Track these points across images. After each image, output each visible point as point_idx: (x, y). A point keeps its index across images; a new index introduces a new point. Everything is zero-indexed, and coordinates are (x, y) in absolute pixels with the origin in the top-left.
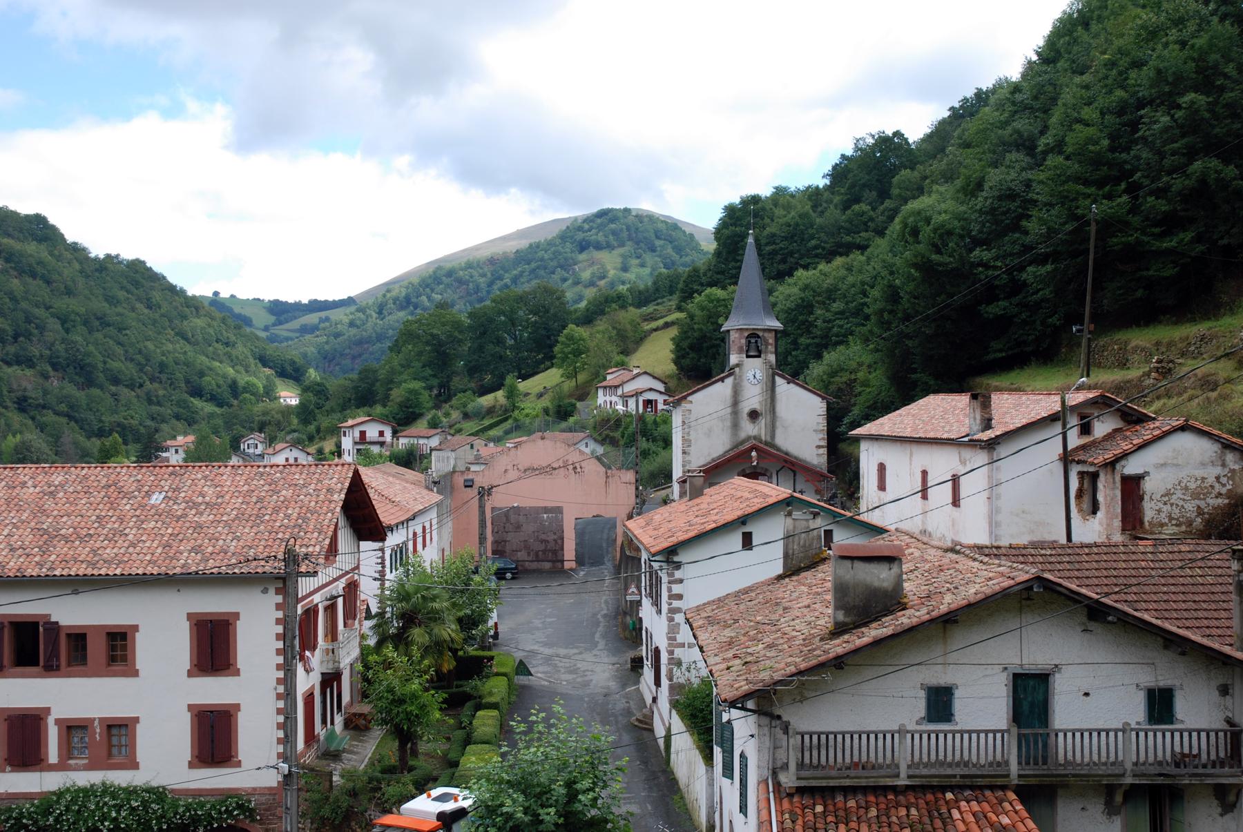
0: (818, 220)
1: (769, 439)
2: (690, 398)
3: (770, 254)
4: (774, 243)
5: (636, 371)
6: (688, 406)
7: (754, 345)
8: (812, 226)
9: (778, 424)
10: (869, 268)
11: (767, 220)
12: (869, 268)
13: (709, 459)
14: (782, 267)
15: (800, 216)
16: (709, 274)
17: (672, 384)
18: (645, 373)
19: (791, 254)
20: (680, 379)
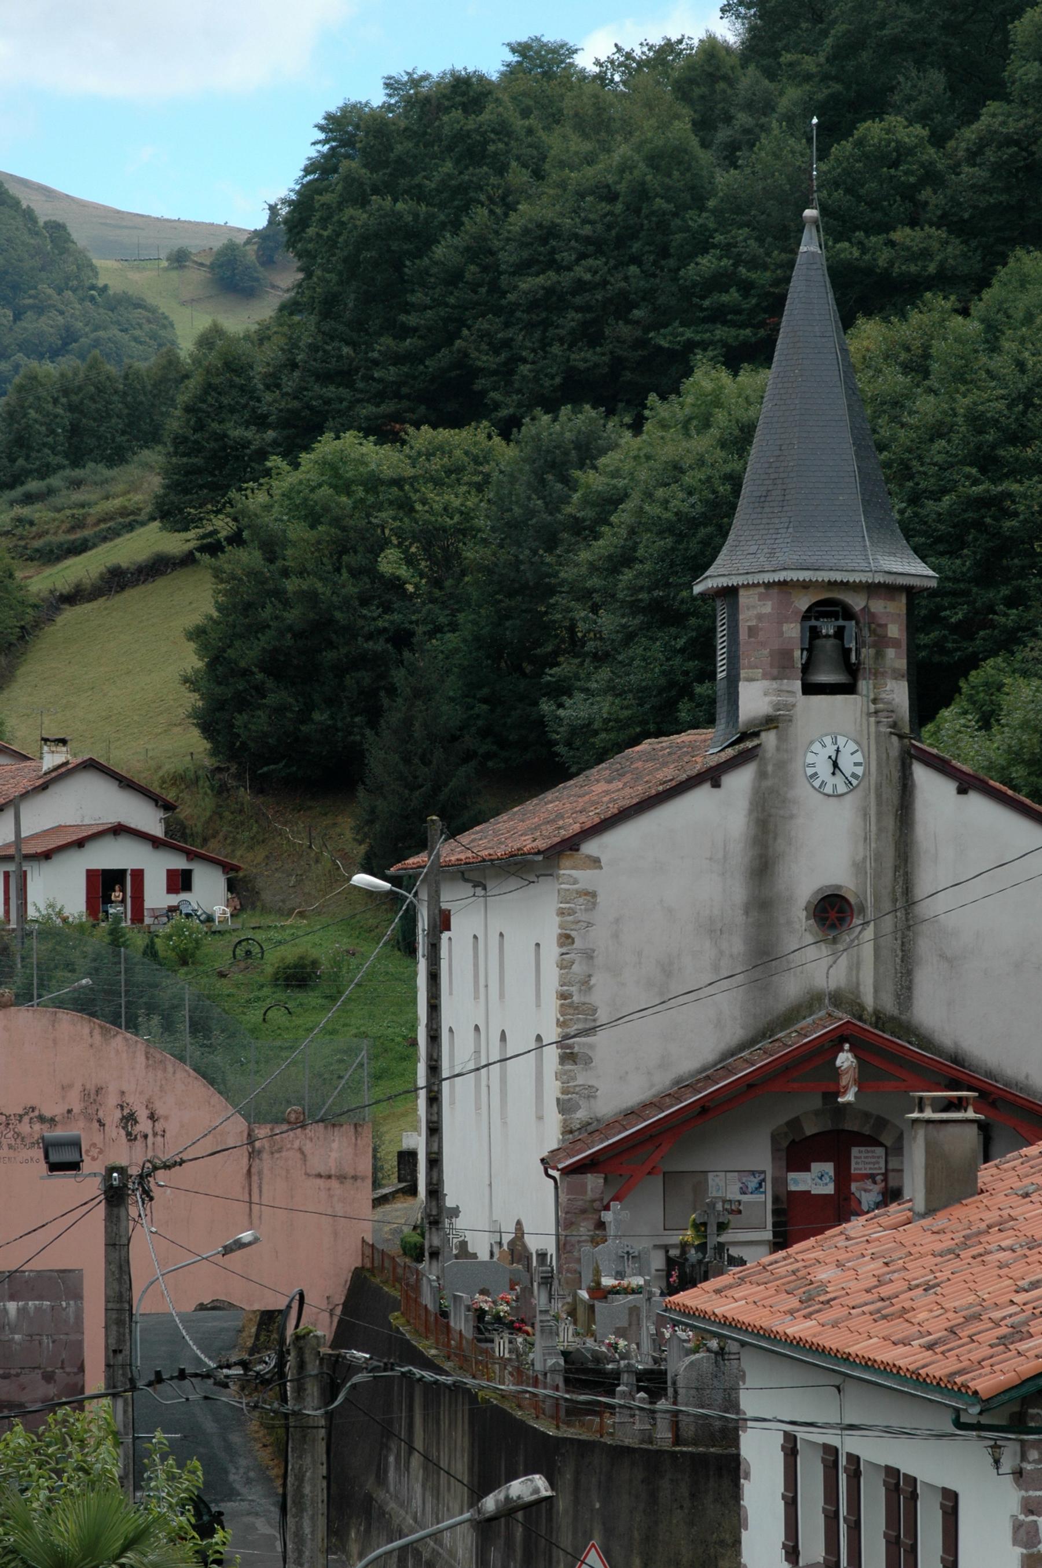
0: (724, 179)
1: (889, 1006)
2: (591, 848)
3: (534, 305)
4: (552, 264)
5: (52, 759)
6: (584, 877)
7: (829, 647)
8: (699, 202)
9: (924, 947)
10: (999, 363)
11: (518, 176)
12: (999, 363)
13: (663, 1081)
14: (583, 357)
15: (654, 160)
16: (290, 382)
17: (196, 808)
18: (91, 765)
19: (621, 306)
20: (221, 790)
